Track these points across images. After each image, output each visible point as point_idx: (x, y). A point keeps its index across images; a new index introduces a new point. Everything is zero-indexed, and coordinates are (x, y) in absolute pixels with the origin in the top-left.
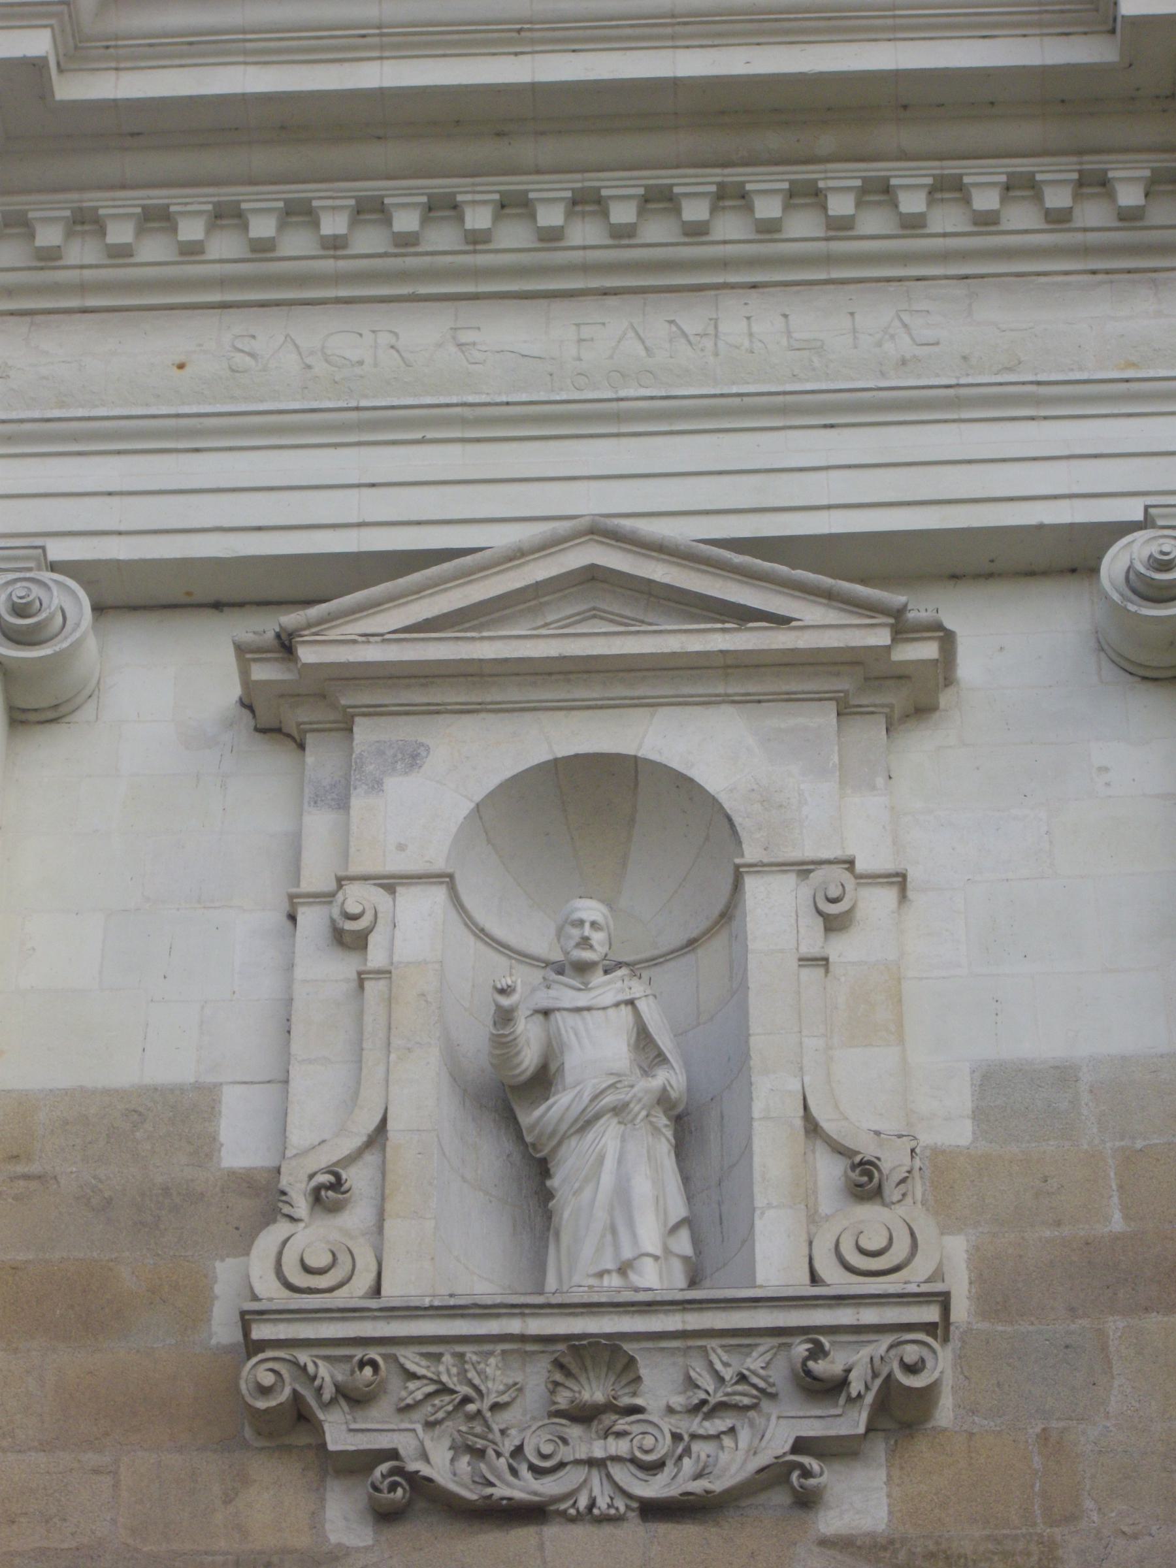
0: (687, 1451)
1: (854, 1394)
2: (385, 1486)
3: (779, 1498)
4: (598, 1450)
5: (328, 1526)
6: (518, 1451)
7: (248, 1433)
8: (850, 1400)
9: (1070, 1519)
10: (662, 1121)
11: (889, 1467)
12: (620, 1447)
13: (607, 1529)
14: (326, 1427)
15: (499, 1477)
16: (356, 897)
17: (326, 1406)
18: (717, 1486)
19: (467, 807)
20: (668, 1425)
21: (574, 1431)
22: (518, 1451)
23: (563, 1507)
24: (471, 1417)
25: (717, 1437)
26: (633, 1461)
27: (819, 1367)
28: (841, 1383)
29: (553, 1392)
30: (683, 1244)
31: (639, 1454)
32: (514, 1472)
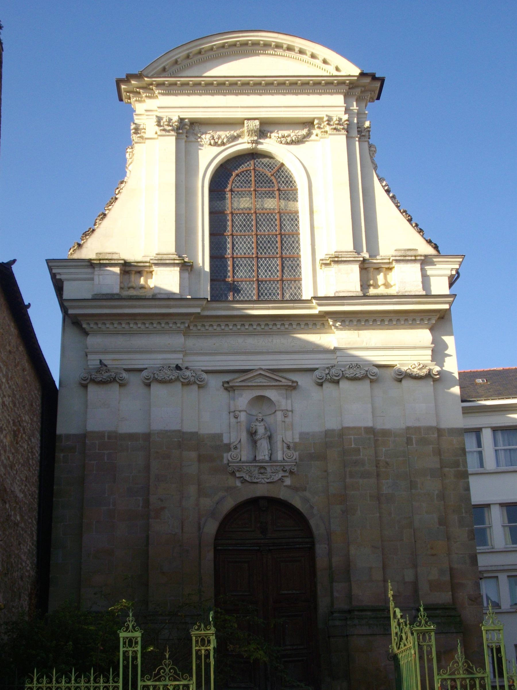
4: (263, 477)
10: (268, 438)
16: (237, 413)
19: (247, 401)
21: (260, 475)
27: (284, 469)
28: (286, 471)
30: (270, 452)
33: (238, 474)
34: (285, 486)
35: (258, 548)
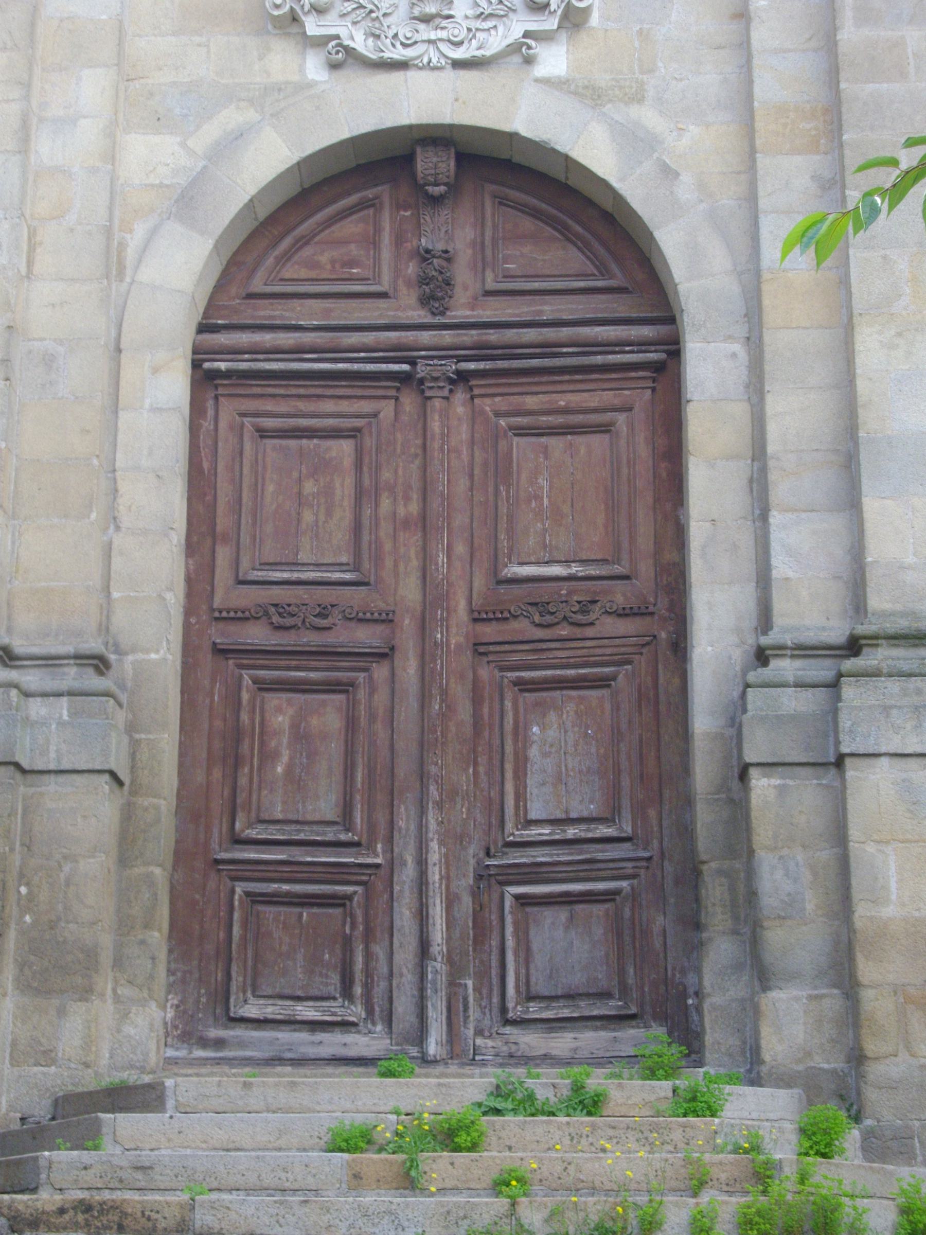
0: (474, 36)
1: (552, 10)
2: (333, 52)
3: (516, 59)
4: (433, 36)
5: (307, 71)
6: (396, 36)
7: (270, 27)
8: (550, 13)
9: (651, 71)
11: (568, 45)
12: (442, 34)
13: (436, 73)
14: (306, 24)
15: (387, 48)
17: (305, 14)
18: (488, 53)
20: (465, 24)
21: (422, 27)
22: (396, 36)
23: (416, 62)
24: (374, 20)
25: (488, 30)
26: (449, 41)
29: (412, 8)
31: (452, 38)
32: (393, 45)
33: (313, 26)
34: (537, 80)
35: (405, 367)
